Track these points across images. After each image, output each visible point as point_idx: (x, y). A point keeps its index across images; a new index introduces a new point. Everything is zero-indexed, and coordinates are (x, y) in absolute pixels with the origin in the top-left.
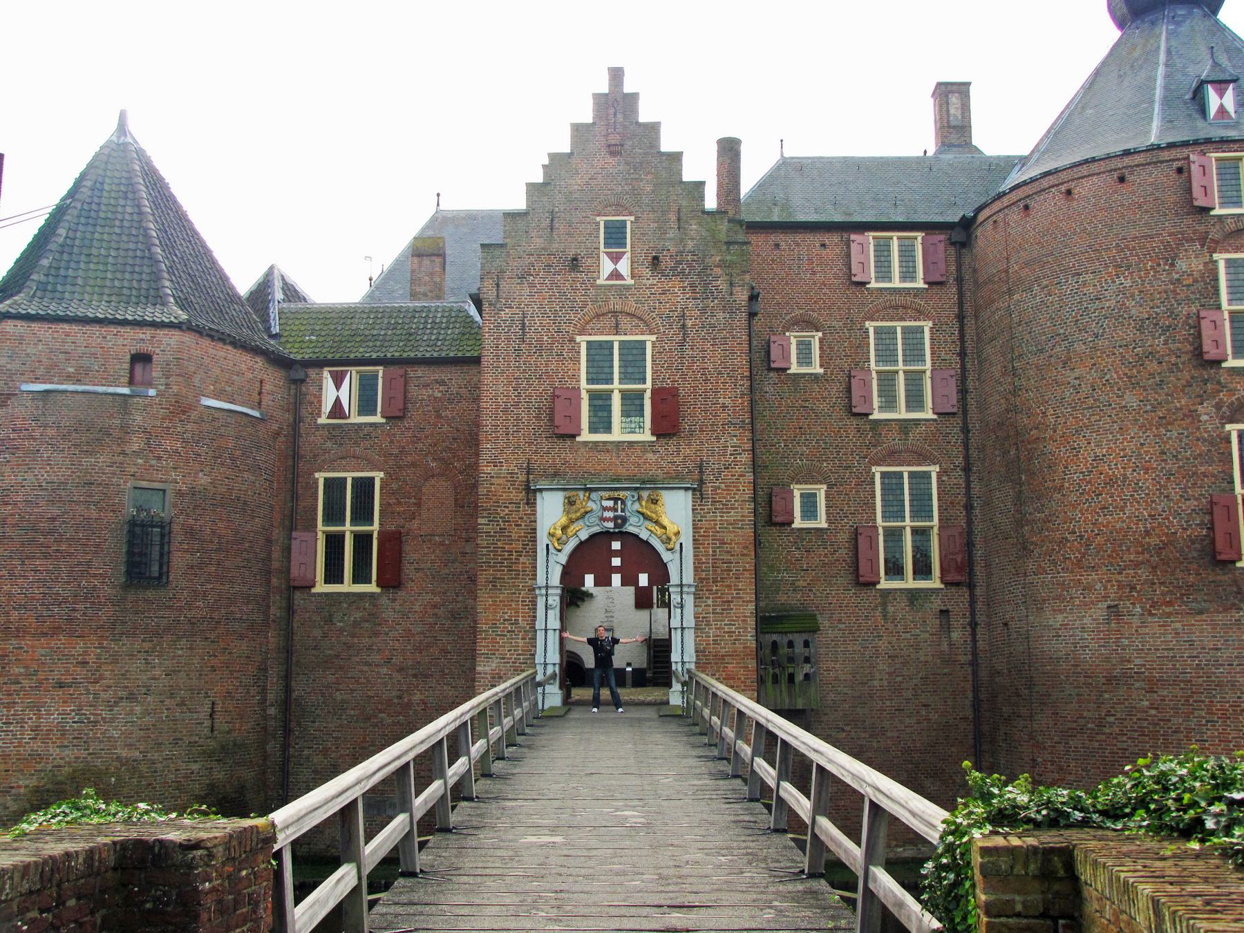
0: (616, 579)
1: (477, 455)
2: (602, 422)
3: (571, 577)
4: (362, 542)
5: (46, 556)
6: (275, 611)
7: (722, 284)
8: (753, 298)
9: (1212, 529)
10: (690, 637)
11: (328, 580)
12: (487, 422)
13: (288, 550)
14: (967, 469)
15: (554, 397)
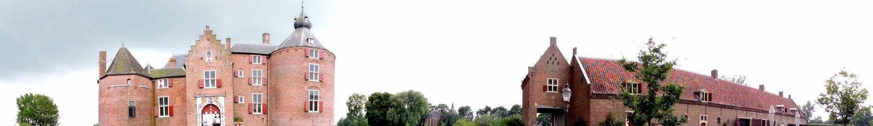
0: (211, 112)
1: (186, 92)
2: (207, 85)
3: (203, 112)
4: (166, 108)
5: (117, 113)
6: (152, 121)
7: (228, 62)
8: (233, 64)
9: (305, 105)
10: (224, 122)
11: (161, 115)
12: (187, 85)
13: (154, 110)
14: (267, 94)
15: (199, 81)
